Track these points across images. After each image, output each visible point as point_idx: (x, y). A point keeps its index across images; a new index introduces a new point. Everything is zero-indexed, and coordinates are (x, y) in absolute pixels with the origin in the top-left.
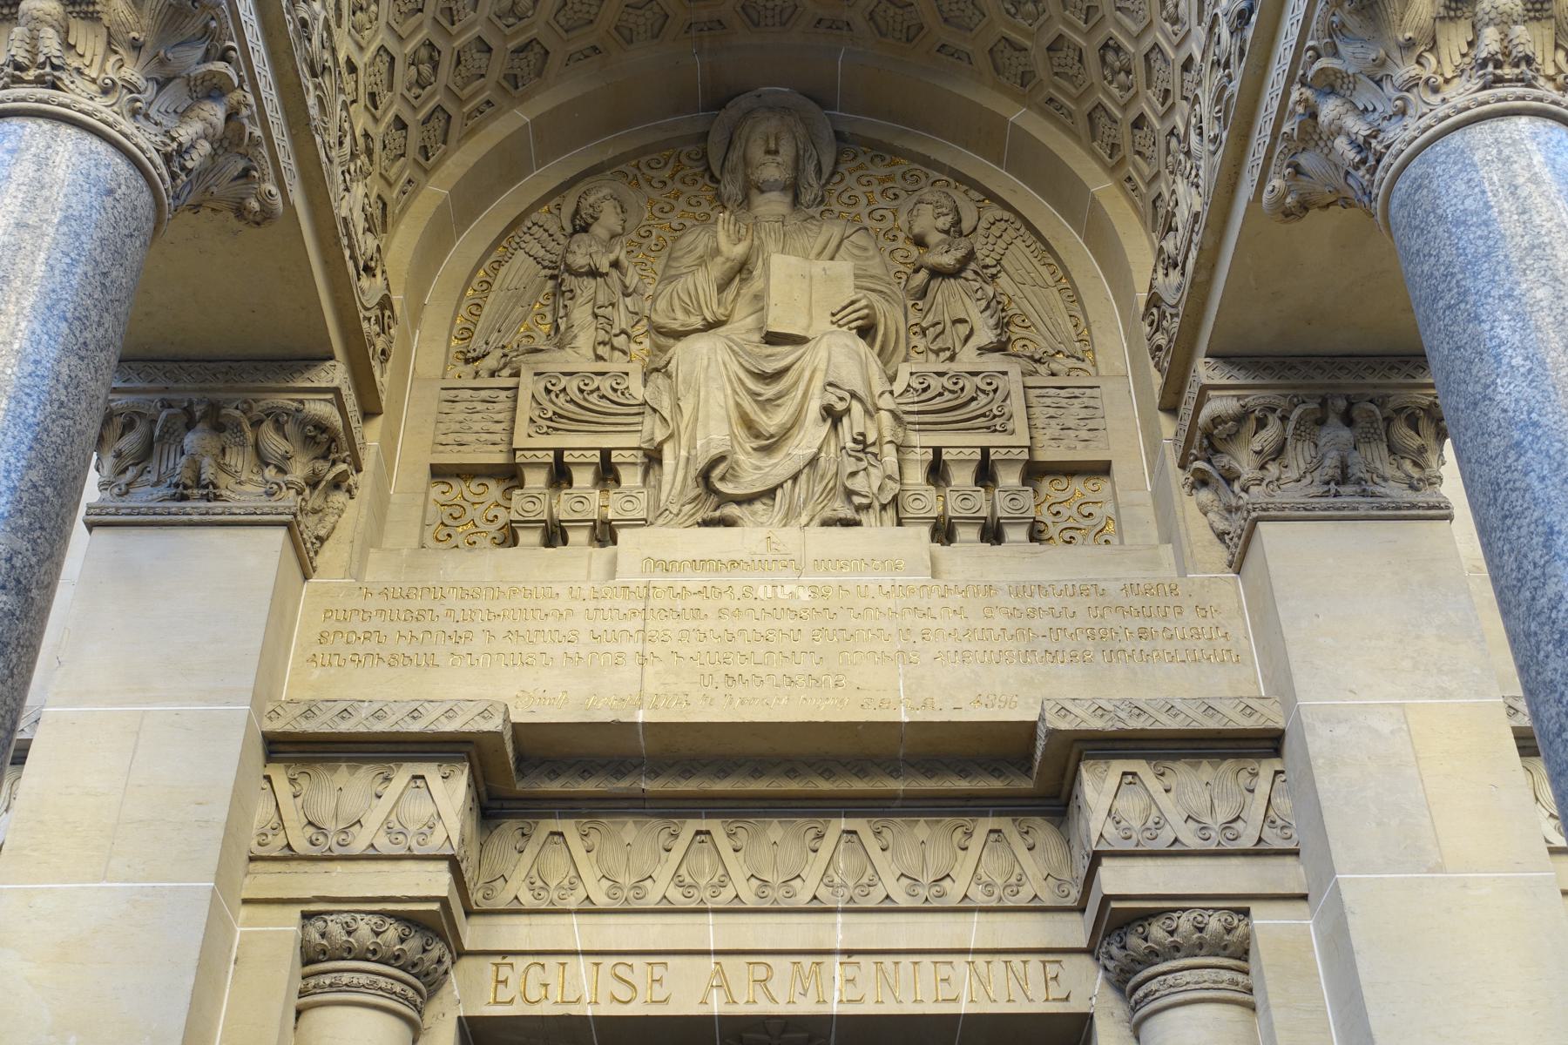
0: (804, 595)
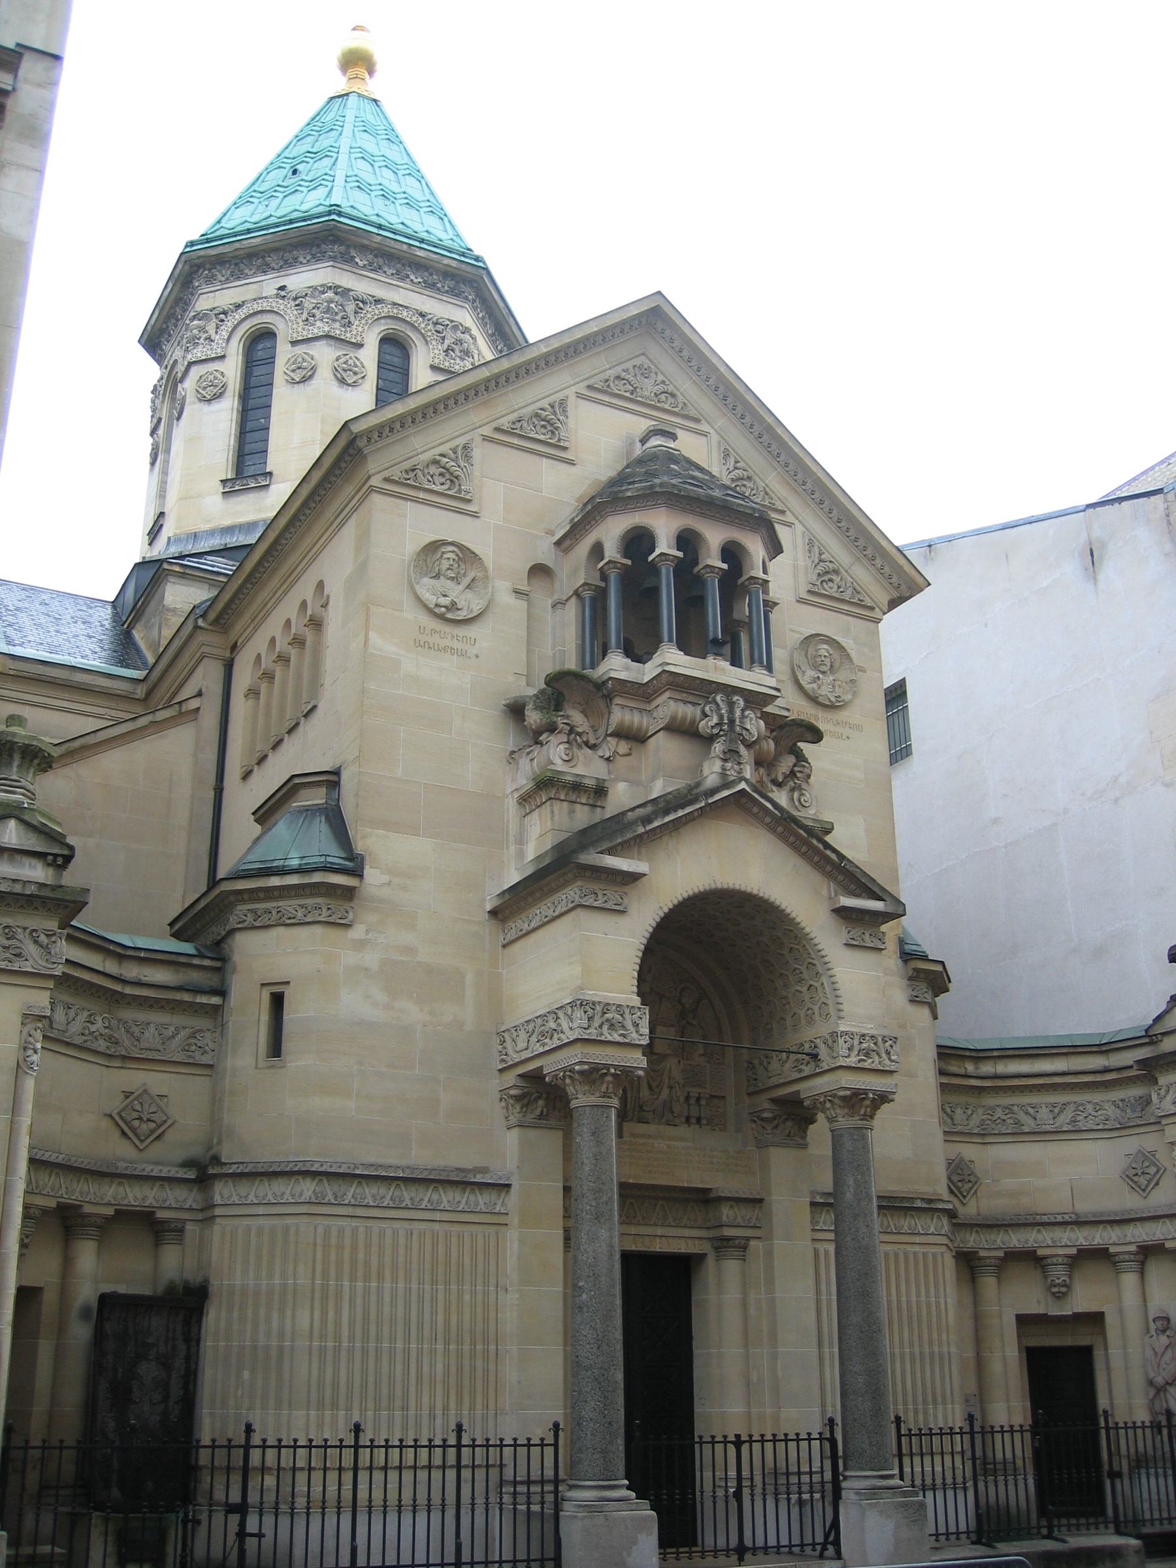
0: (665, 1147)
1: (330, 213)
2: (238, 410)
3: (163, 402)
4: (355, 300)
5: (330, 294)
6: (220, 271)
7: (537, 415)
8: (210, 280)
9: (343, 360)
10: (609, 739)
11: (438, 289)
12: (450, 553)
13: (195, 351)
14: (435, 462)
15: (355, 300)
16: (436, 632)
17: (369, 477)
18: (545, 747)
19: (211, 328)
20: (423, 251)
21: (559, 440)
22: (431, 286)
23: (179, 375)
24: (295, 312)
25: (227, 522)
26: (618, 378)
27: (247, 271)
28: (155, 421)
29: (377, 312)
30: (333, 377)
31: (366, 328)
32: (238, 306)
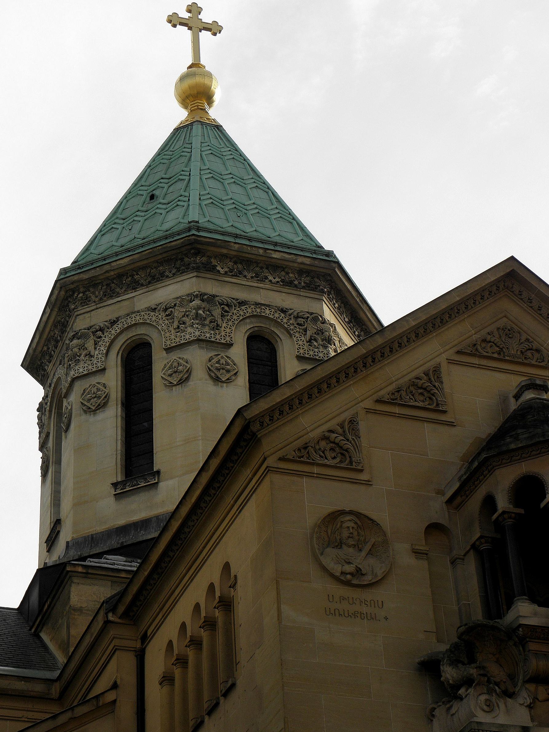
1: (189, 229)
2: (122, 417)
3: (50, 417)
4: (221, 304)
5: (197, 302)
6: (94, 293)
7: (414, 384)
8: (86, 301)
9: (216, 359)
10: (527, 686)
11: (296, 286)
12: (348, 522)
13: (77, 367)
14: (325, 438)
15: (221, 304)
16: (344, 599)
17: (265, 459)
18: (465, 701)
19: (90, 345)
20: (277, 253)
21: (438, 405)
22: (289, 284)
23: (64, 391)
24: (166, 322)
25: (121, 522)
26: (484, 341)
27: (118, 290)
28: (44, 436)
29: (242, 313)
30: (207, 377)
31: (233, 328)
32: (113, 323)
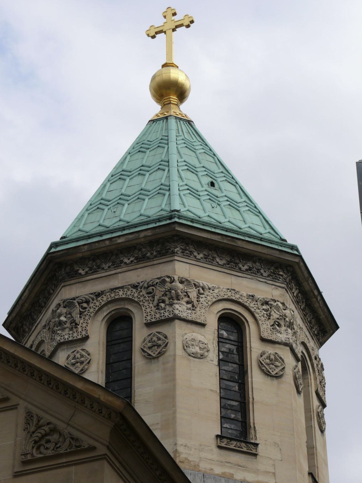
9: (72, 356)
11: (148, 258)
